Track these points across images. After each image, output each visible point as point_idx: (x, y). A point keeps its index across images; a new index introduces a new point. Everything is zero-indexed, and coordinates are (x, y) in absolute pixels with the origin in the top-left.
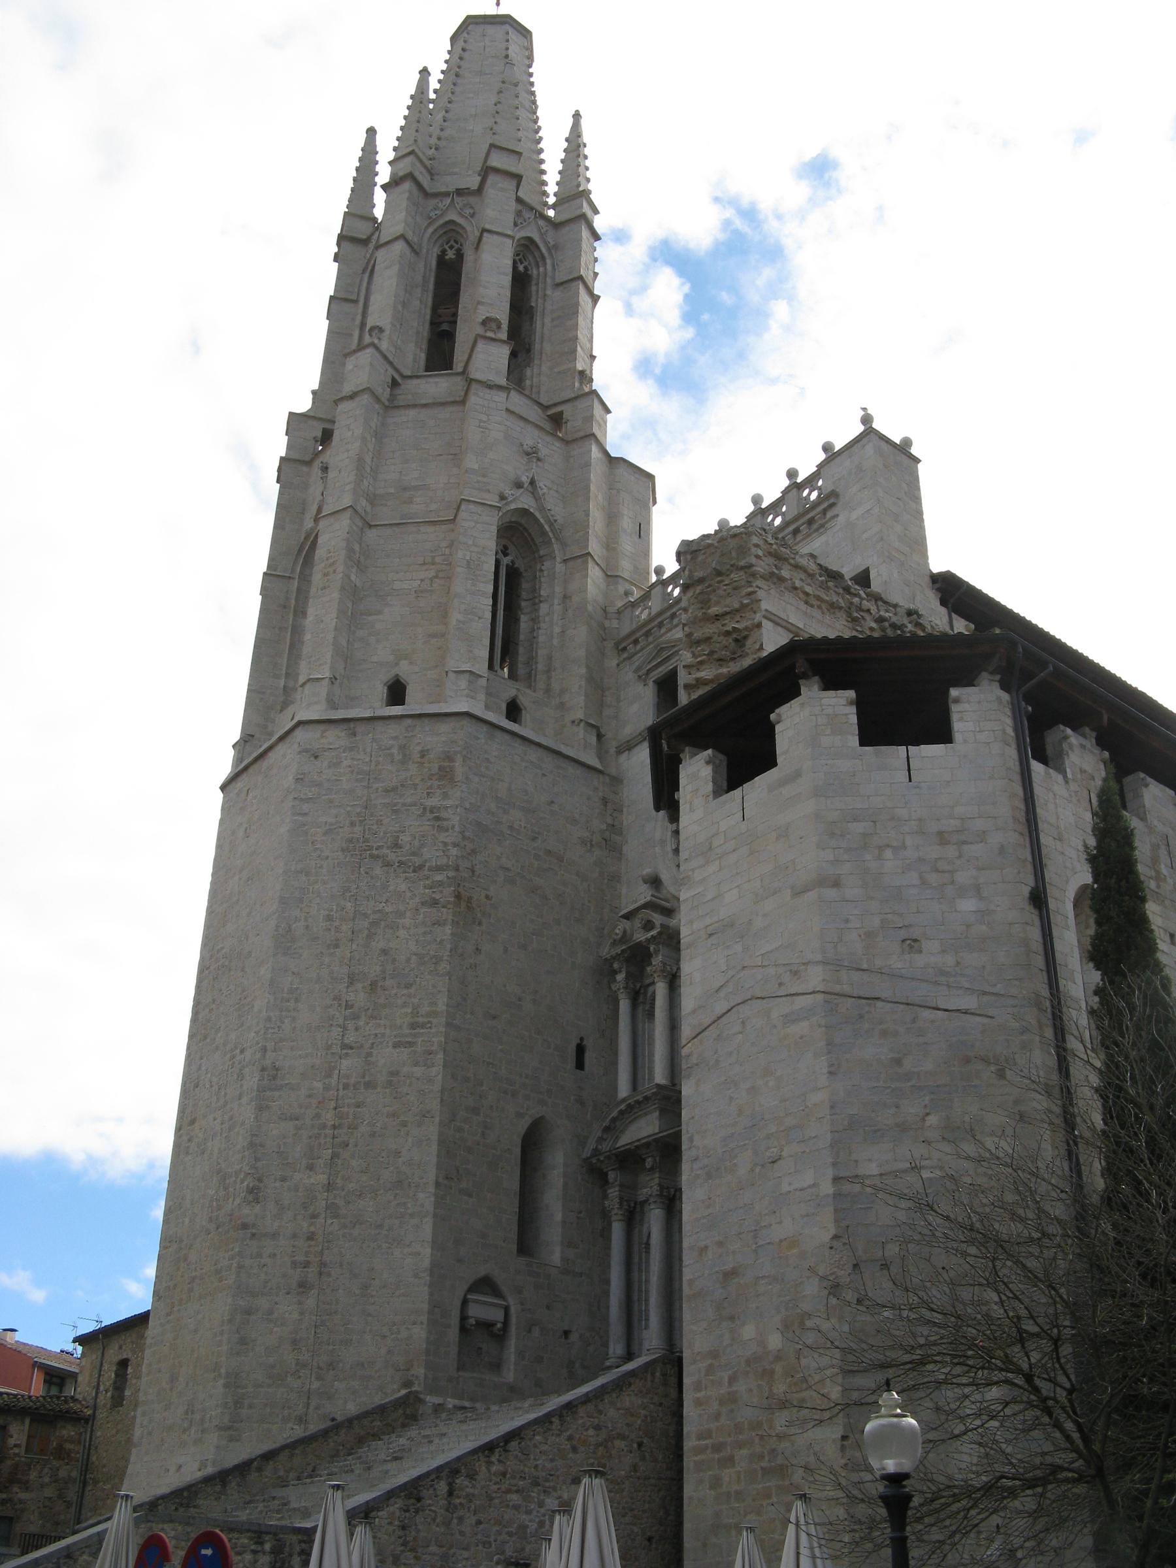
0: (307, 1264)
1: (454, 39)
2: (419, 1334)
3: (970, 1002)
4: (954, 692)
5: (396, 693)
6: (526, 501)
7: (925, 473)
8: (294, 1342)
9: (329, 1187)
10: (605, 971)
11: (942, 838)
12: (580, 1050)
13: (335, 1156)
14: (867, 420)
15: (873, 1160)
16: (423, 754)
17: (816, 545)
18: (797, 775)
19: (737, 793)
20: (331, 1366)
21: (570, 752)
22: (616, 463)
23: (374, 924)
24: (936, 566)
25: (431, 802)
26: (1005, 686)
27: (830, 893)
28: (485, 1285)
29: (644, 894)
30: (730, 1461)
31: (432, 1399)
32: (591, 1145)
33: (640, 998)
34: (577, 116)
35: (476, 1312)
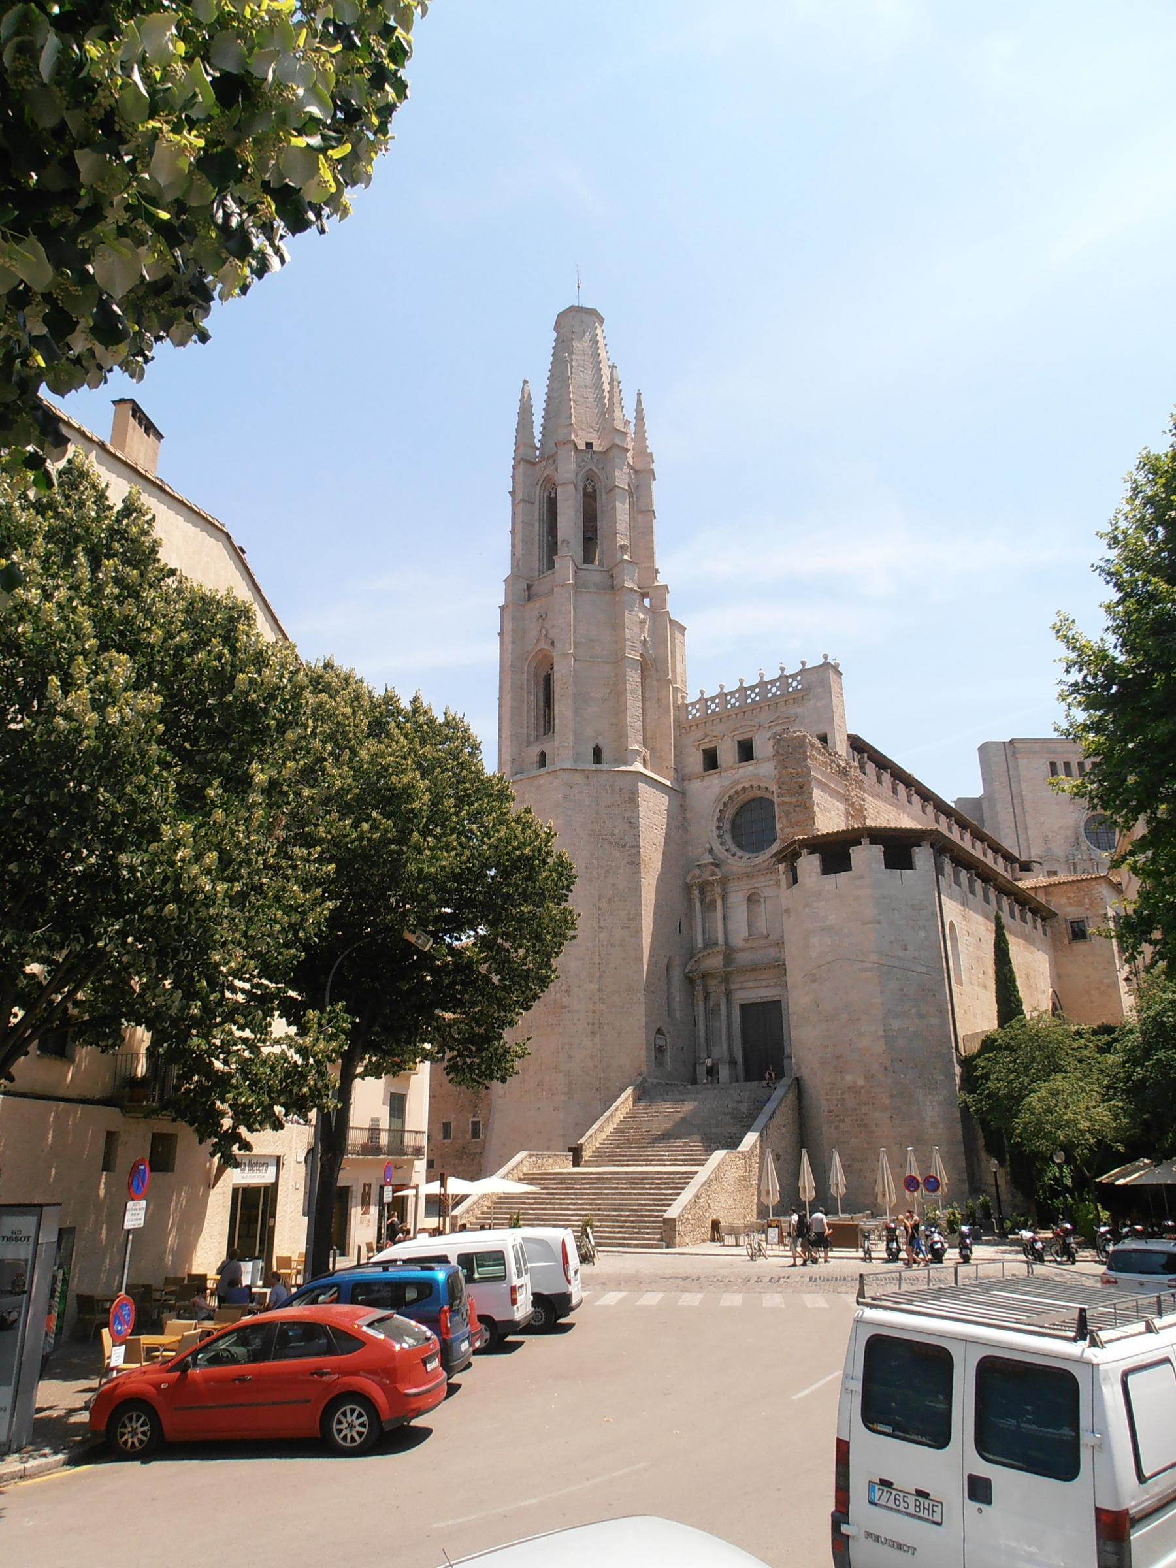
0: (593, 1024)
1: (561, 315)
2: (643, 1053)
3: (924, 970)
4: (916, 849)
8: (592, 1057)
9: (600, 990)
11: (913, 907)
13: (601, 977)
14: (826, 656)
15: (896, 1024)
17: (799, 710)
18: (862, 877)
20: (608, 1067)
23: (607, 871)
25: (627, 814)
26: (932, 846)
27: (877, 926)
28: (659, 1031)
29: (708, 859)
30: (843, 1121)
31: (650, 1080)
32: (689, 967)
34: (639, 394)
35: (660, 1042)
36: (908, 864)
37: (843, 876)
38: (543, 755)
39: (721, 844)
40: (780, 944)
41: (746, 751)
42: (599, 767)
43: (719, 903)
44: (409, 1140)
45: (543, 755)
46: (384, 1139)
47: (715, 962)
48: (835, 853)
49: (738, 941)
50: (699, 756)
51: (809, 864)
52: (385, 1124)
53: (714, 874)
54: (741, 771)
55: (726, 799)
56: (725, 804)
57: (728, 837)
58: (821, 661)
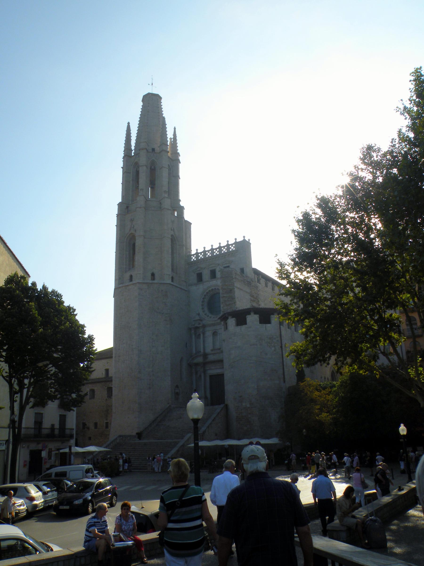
4: (272, 316)
5: (153, 275)
6: (172, 233)
7: (252, 246)
10: (190, 329)
12: (186, 344)
14: (244, 237)
16: (162, 291)
19: (240, 327)
21: (183, 288)
22: (186, 221)
24: (254, 266)
28: (177, 386)
29: (197, 318)
33: (198, 337)
34: (175, 128)
36: (269, 322)
37: (244, 327)
38: (131, 277)
39: (203, 312)
40: (222, 352)
41: (213, 274)
42: (153, 282)
43: (202, 335)
44: (68, 432)
45: (131, 277)
46: (57, 432)
47: (200, 360)
48: (241, 317)
49: (208, 350)
50: (195, 276)
51: (231, 322)
52: (57, 426)
53: (199, 324)
54: (211, 282)
55: (205, 293)
56: (205, 295)
57: (206, 309)
58: (242, 239)
